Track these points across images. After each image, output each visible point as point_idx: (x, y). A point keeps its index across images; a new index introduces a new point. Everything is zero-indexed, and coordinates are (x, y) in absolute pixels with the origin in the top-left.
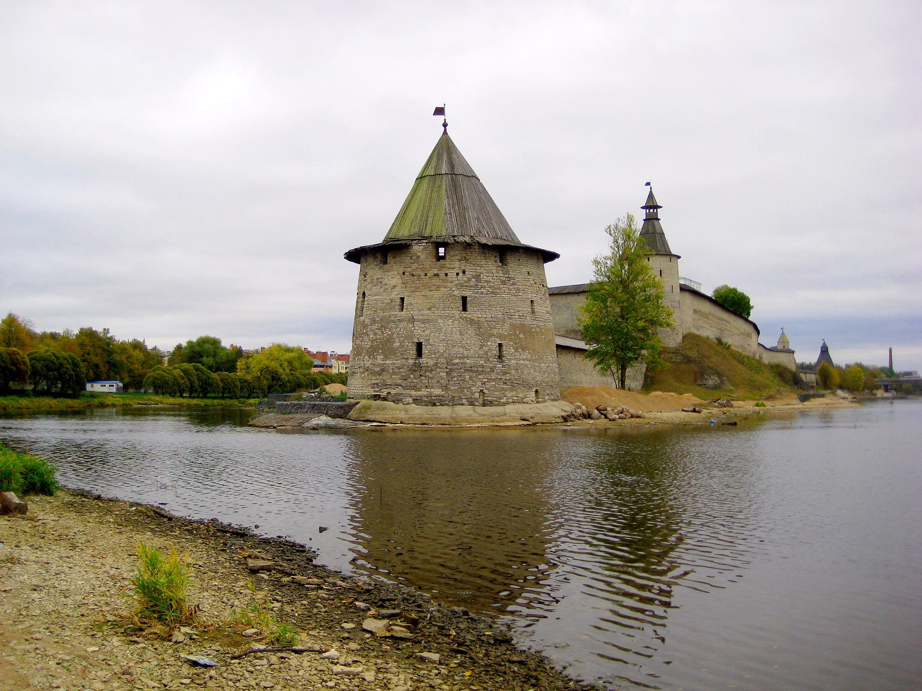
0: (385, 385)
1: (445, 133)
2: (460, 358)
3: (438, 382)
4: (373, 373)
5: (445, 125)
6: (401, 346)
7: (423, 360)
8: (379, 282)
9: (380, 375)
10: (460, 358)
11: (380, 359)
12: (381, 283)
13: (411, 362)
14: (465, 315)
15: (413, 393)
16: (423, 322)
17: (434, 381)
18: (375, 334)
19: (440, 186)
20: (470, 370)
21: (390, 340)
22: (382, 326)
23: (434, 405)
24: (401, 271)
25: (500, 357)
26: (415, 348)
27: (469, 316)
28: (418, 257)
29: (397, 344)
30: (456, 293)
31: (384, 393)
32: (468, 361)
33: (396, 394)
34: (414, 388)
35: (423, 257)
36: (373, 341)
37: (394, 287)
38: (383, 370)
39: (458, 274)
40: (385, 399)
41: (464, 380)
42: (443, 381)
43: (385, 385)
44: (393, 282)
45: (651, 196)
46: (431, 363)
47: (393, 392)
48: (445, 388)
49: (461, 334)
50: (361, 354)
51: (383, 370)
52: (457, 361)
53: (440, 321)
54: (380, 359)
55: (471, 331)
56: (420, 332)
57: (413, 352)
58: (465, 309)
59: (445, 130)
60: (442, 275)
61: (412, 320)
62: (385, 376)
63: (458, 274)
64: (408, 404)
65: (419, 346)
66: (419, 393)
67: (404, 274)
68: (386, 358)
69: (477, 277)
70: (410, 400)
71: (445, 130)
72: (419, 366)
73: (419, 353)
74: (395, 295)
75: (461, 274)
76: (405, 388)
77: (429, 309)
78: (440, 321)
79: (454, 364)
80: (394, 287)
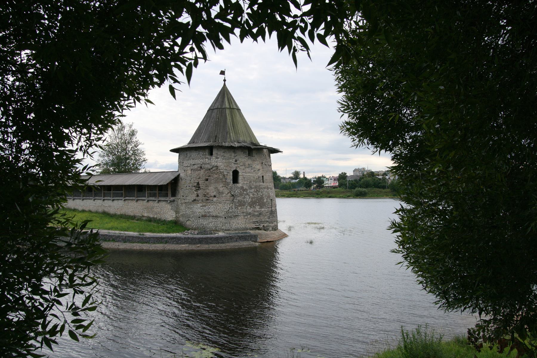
0: (262, 222)
4: (254, 215)
5: (225, 80)
8: (250, 166)
9: (259, 216)
18: (253, 195)
21: (262, 198)
22: (257, 190)
29: (265, 200)
31: (261, 226)
33: (267, 226)
36: (252, 198)
37: (259, 170)
38: (260, 214)
40: (261, 230)
43: (262, 222)
47: (265, 225)
50: (244, 205)
51: (260, 214)
54: (257, 208)
59: (225, 83)
62: (262, 217)
68: (261, 207)
71: (225, 83)
74: (260, 174)
80: (259, 170)
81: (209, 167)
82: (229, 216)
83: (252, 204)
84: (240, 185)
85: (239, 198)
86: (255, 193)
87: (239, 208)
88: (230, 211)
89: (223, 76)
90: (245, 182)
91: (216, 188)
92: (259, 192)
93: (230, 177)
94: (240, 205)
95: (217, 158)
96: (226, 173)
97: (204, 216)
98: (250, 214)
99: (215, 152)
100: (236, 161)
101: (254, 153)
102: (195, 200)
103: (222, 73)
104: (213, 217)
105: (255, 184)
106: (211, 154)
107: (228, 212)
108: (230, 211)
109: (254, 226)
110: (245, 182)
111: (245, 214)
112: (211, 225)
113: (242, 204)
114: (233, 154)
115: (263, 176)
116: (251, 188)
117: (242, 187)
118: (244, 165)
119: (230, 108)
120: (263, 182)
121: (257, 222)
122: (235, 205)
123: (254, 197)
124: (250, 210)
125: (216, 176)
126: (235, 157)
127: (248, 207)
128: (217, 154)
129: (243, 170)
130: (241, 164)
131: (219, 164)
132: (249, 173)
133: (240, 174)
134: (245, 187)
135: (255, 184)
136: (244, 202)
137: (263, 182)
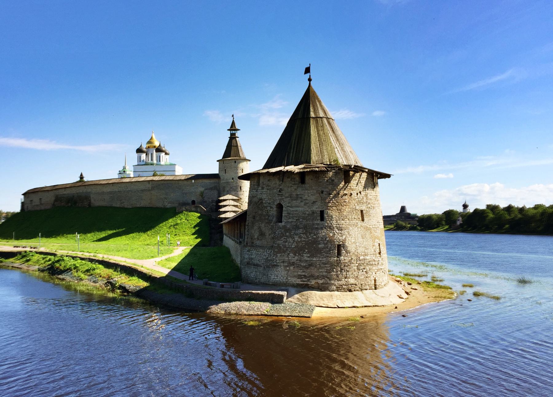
2: (363, 255)
4: (299, 266)
5: (310, 80)
6: (324, 248)
8: (297, 197)
9: (307, 268)
10: (363, 255)
11: (306, 257)
14: (363, 224)
15: (336, 283)
17: (350, 273)
23: (350, 291)
25: (380, 253)
28: (333, 180)
30: (357, 208)
31: (313, 282)
32: (368, 258)
35: (336, 181)
37: (314, 202)
38: (311, 265)
39: (357, 194)
43: (312, 277)
44: (313, 198)
45: (233, 123)
46: (347, 259)
47: (321, 282)
49: (363, 238)
50: (284, 252)
52: (361, 258)
53: (351, 228)
54: (306, 257)
55: (368, 235)
56: (338, 237)
58: (363, 220)
62: (314, 271)
63: (357, 194)
64: (333, 291)
68: (312, 256)
70: (335, 288)
72: (339, 263)
73: (339, 254)
74: (316, 208)
80: (314, 202)
81: (255, 200)
82: (271, 265)
83: (298, 251)
84: (283, 224)
87: (279, 255)
88: (269, 258)
89: (307, 75)
90: (290, 220)
91: (260, 228)
92: (310, 233)
93: (274, 212)
94: (279, 252)
95: (263, 188)
97: (248, 263)
98: (293, 264)
99: (262, 180)
100: (280, 191)
102: (247, 244)
103: (307, 70)
104: (254, 265)
105: (304, 222)
107: (267, 260)
109: (299, 281)
110: (290, 220)
112: (252, 275)
113: (281, 250)
114: (278, 182)
116: (297, 227)
117: (284, 227)
118: (290, 196)
121: (305, 276)
123: (301, 241)
125: (260, 212)
126: (280, 185)
129: (289, 203)
130: (287, 195)
131: (264, 196)
132: (297, 207)
133: (284, 209)
135: (304, 222)
136: (285, 246)
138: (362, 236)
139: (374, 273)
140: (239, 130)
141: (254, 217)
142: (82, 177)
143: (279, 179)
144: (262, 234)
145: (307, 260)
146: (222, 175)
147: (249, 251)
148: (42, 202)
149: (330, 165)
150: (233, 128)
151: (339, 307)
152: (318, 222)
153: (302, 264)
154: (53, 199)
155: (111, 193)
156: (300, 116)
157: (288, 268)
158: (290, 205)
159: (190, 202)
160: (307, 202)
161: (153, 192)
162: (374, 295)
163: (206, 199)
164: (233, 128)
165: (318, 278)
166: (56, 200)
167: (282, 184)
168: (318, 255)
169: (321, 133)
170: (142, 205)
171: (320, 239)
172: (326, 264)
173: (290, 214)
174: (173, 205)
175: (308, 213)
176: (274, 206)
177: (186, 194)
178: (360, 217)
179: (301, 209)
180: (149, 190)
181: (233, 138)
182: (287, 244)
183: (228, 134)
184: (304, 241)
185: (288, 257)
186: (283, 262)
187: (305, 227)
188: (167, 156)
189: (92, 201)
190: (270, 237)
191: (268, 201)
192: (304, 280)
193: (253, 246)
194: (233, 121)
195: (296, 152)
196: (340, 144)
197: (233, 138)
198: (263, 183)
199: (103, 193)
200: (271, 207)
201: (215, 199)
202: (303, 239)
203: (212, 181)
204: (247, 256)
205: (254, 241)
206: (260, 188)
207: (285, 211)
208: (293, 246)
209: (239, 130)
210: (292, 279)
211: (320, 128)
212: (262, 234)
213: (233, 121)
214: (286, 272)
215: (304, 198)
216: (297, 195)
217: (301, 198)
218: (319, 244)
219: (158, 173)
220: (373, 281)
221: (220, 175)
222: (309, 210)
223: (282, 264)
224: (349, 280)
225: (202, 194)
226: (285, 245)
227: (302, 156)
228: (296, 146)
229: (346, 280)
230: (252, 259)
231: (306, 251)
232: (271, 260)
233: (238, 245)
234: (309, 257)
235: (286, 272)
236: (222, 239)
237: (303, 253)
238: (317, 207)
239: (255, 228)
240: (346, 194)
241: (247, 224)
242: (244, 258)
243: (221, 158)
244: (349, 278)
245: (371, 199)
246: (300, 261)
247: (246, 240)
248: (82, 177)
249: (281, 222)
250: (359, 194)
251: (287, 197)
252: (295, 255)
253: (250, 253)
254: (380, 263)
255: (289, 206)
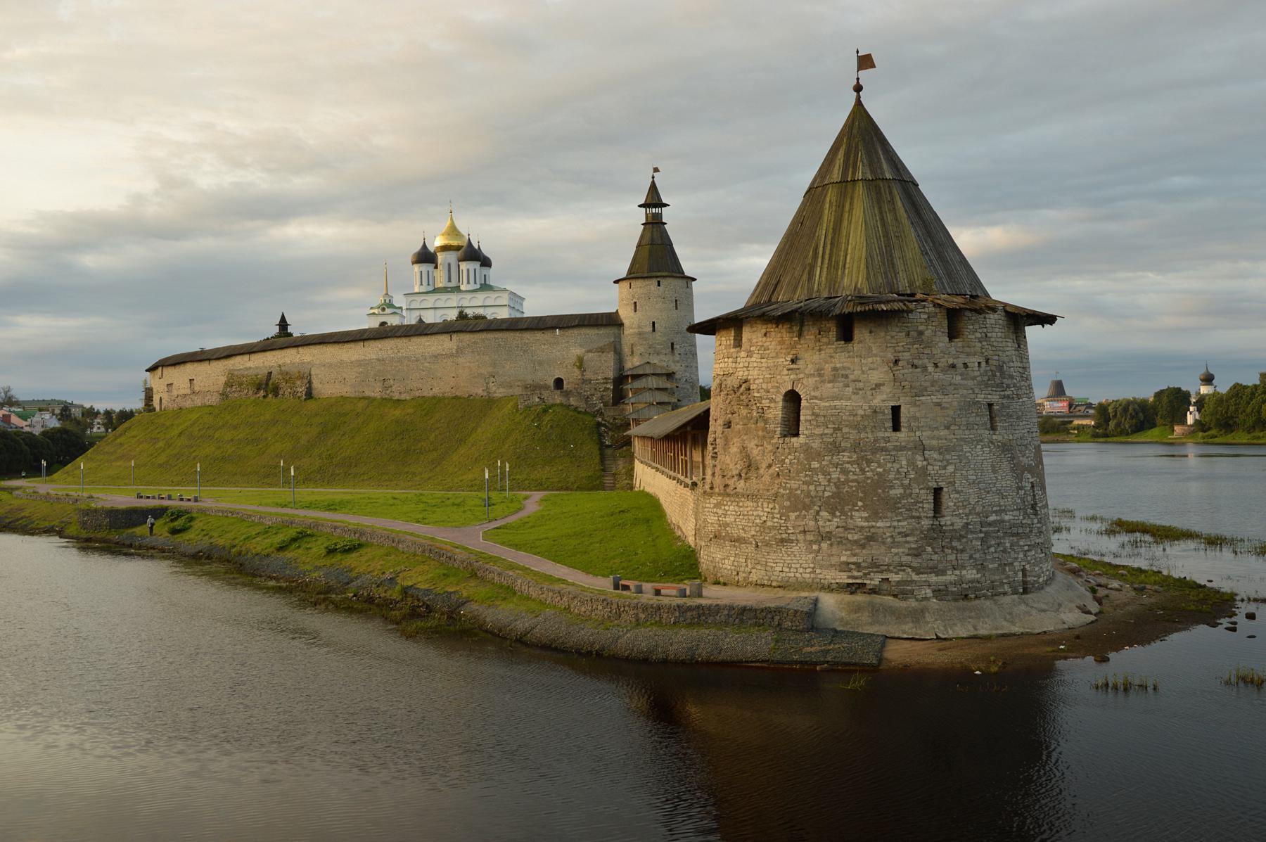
0: (875, 566)
1: (859, 103)
2: (996, 512)
3: (971, 557)
4: (842, 542)
5: (858, 88)
6: (903, 496)
7: (947, 520)
9: (863, 546)
10: (996, 512)
12: (846, 377)
13: (926, 523)
15: (933, 578)
16: (940, 450)
17: (965, 556)
18: (845, 472)
19: (892, 201)
20: (1014, 532)
24: (891, 357)
25: (1033, 507)
26: (931, 498)
27: (1000, 438)
28: (921, 333)
30: (981, 398)
31: (874, 580)
32: (1007, 518)
34: (935, 570)
38: (871, 538)
40: (874, 591)
41: (1004, 551)
42: (977, 556)
43: (875, 566)
44: (875, 377)
45: (653, 188)
46: (959, 523)
47: (894, 578)
48: (981, 567)
49: (995, 472)
50: (806, 507)
52: (993, 518)
53: (966, 448)
54: (859, 518)
55: (1005, 465)
57: (929, 506)
58: (993, 428)
59: (858, 98)
60: (960, 365)
61: (921, 448)
62: (876, 550)
65: (937, 492)
66: (942, 579)
67: (896, 362)
68: (875, 515)
69: (1000, 368)
70: (929, 593)
71: (858, 98)
74: (883, 400)
75: (983, 364)
76: (918, 571)
77: (948, 428)
78: (966, 448)
79: (990, 524)
80: (878, 386)
81: (732, 382)
84: (801, 439)
85: (794, 484)
86: (855, 468)
87: (793, 516)
88: (769, 524)
92: (869, 462)
93: (776, 412)
94: (794, 508)
96: (765, 403)
98: (828, 536)
99: (747, 334)
100: (793, 361)
101: (860, 333)
102: (712, 488)
105: (853, 435)
106: (738, 343)
108: (769, 524)
109: (843, 578)
111: (810, 537)
112: (728, 565)
115: (896, 410)
116: (836, 448)
117: (807, 449)
119: (844, 181)
120: (896, 427)
121: (858, 565)
122: (782, 507)
123: (847, 481)
124: (830, 523)
127: (824, 514)
128: (750, 340)
129: (816, 388)
131: (753, 374)
133: (804, 403)
134: (816, 445)
135: (853, 435)
136: (808, 495)
137: (896, 427)
138: (993, 466)
139: (1021, 555)
140: (666, 205)
141: (728, 425)
142: (283, 324)
143: (790, 331)
144: (750, 466)
145: (862, 527)
146: (626, 315)
147: (717, 505)
148: (197, 389)
149: (913, 295)
150: (654, 201)
151: (938, 638)
152: (887, 434)
153: (850, 537)
154: (223, 379)
155: (359, 363)
156: (836, 175)
157: (815, 547)
158: (817, 394)
159: (551, 382)
160: (861, 385)
161: (461, 360)
162: (1023, 607)
163: (588, 375)
164: (654, 201)
165: (888, 568)
166: (228, 384)
167: (798, 342)
168: (889, 514)
169: (889, 217)
170: (436, 391)
171: (891, 476)
172: (906, 536)
173: (817, 416)
174: (510, 392)
175: (861, 412)
176: (780, 398)
177: (540, 363)
178: (986, 419)
179: (844, 403)
180: (452, 356)
181: (655, 226)
182: (812, 488)
183: (641, 216)
184: (853, 481)
185: (817, 521)
186: (805, 532)
187: (856, 447)
188: (485, 270)
189: (316, 384)
190: (771, 471)
191: (764, 386)
192: (856, 574)
193: (728, 495)
194: (653, 183)
195: (830, 264)
196: (934, 243)
197: (655, 226)
198: (750, 340)
199: (341, 363)
200: (772, 400)
201: (611, 375)
202: (852, 477)
203: (602, 331)
204: (712, 519)
205: (731, 482)
206: (743, 354)
207: (807, 408)
208: (827, 494)
209: (666, 205)
210: (825, 572)
211: (886, 207)
212: (750, 466)
213: (653, 183)
214: (811, 556)
215: (851, 377)
216: (835, 369)
217: (846, 377)
218: (892, 487)
219: (470, 312)
220: (1020, 574)
221: (623, 314)
222: (866, 406)
223: (801, 537)
224: (964, 572)
225: (580, 363)
226: (809, 492)
227: (843, 273)
228: (828, 252)
229: (957, 572)
230: (727, 525)
231: (860, 504)
232: (774, 528)
233: (687, 492)
234: (867, 519)
235: (811, 556)
236: (630, 473)
237: (851, 510)
238: (885, 397)
239: (734, 449)
240: (953, 366)
241: (710, 440)
242: (705, 521)
243: (624, 275)
244: (964, 567)
245: (1012, 377)
246: (846, 529)
247: (709, 478)
248: (283, 324)
249: (797, 435)
250: (983, 364)
251: (813, 375)
252: (834, 515)
253: (720, 512)
254: (1035, 531)
255: (816, 398)
